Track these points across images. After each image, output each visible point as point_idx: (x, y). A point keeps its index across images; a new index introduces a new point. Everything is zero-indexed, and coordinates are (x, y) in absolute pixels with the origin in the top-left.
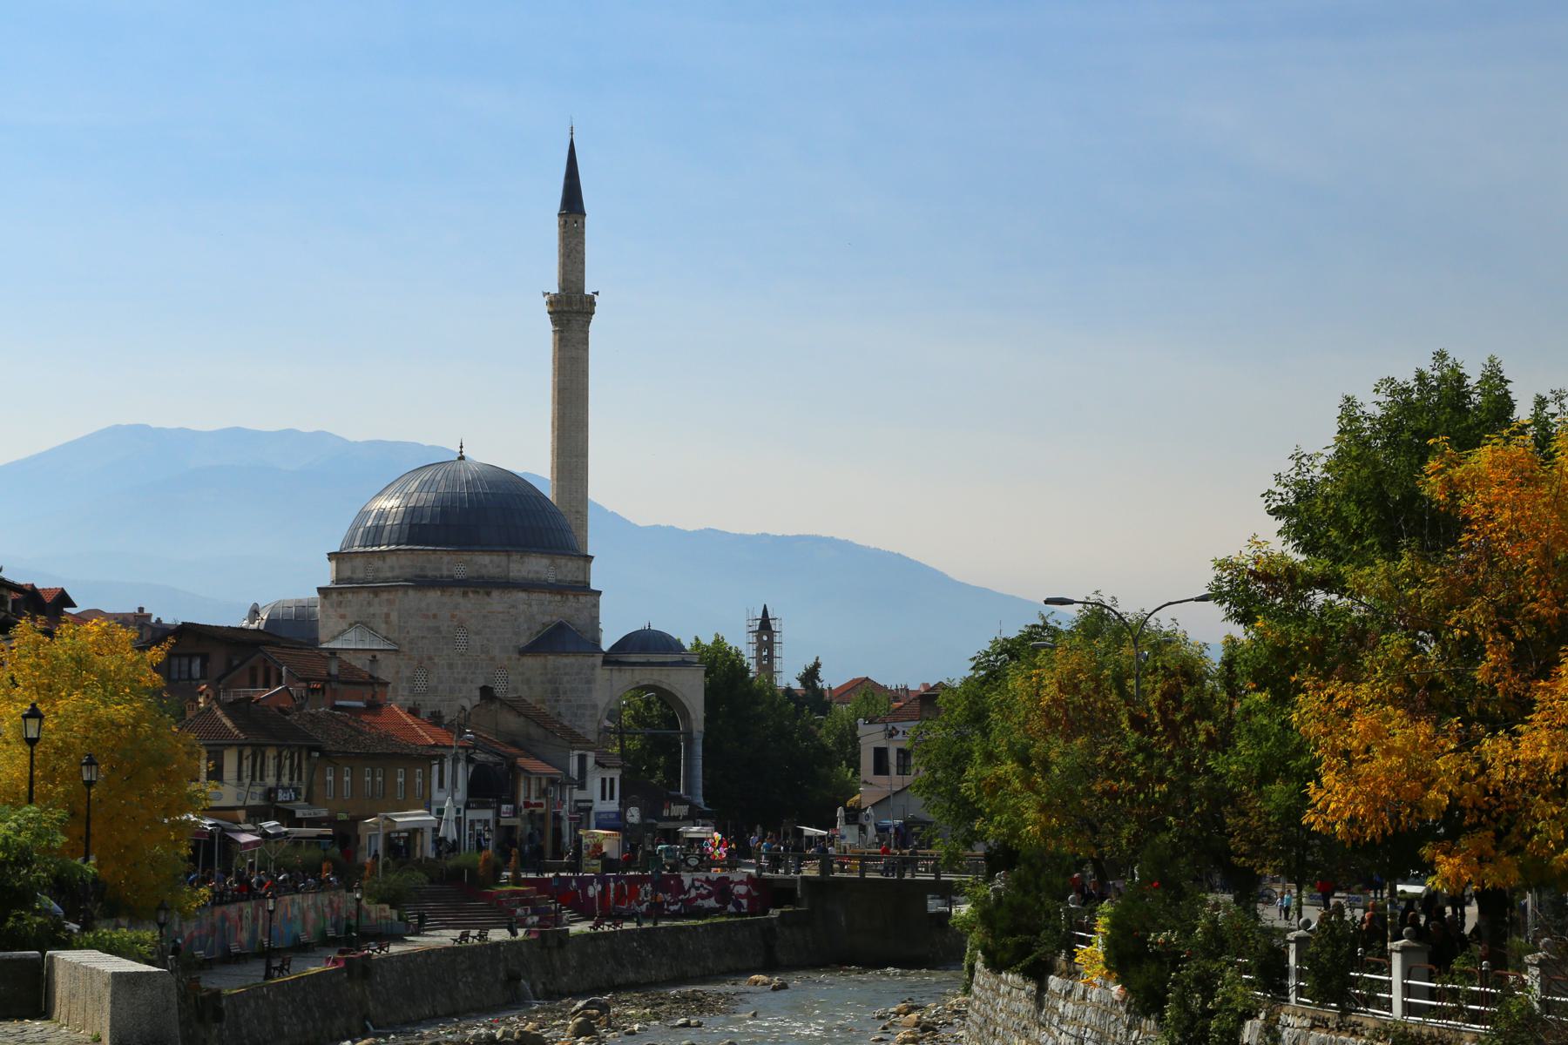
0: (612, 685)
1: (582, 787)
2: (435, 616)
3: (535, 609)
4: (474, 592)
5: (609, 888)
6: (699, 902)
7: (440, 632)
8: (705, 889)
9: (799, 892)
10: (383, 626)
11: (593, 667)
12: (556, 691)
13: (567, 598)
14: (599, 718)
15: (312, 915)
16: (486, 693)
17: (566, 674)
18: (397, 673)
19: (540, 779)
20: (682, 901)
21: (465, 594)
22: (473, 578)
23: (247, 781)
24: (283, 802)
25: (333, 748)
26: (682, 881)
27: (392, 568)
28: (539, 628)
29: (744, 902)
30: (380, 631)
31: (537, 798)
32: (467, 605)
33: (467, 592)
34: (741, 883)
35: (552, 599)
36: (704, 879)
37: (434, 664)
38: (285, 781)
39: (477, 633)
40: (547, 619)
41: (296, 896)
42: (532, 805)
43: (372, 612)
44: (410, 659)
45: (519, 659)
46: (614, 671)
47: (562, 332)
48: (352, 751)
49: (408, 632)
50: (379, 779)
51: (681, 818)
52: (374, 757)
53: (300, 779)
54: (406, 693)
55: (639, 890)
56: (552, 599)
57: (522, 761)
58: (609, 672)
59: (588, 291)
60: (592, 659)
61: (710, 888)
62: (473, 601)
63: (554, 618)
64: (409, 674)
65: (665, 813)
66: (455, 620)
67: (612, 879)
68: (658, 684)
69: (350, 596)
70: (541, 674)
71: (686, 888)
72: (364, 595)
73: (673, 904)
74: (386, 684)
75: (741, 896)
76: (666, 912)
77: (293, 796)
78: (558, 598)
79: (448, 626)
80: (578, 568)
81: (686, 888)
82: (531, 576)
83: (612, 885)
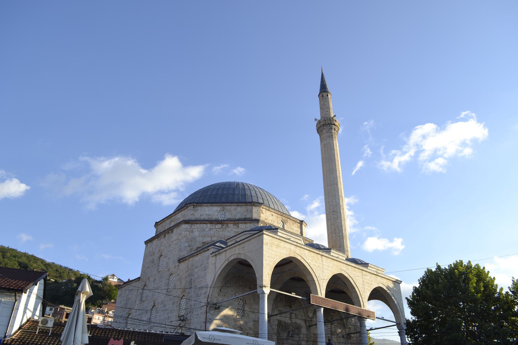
0: (216, 267)
7: (153, 262)
12: (190, 282)
13: (228, 226)
17: (197, 267)
33: (166, 234)
35: (212, 227)
39: (166, 257)
40: (207, 239)
46: (217, 256)
56: (213, 227)
58: (215, 257)
60: (208, 252)
62: (167, 239)
63: (215, 239)
66: (159, 252)
68: (239, 257)
70: (186, 272)
78: (220, 226)
80: (247, 210)
82: (202, 218)
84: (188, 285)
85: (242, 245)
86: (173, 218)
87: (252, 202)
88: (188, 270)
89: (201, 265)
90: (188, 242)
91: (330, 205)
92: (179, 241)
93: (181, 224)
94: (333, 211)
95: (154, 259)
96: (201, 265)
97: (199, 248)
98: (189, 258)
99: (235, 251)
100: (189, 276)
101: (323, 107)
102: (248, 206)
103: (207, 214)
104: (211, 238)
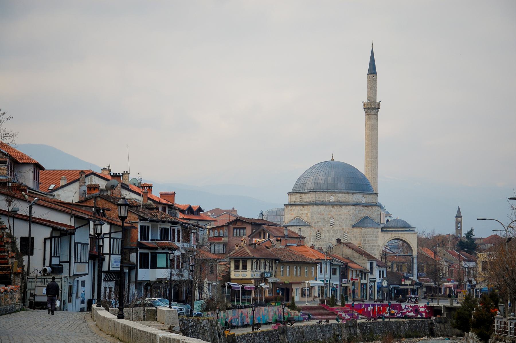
1: (372, 273)
2: (323, 214)
3: (357, 212)
4: (336, 206)
5: (375, 308)
6: (408, 314)
7: (325, 220)
8: (410, 309)
9: (443, 311)
10: (306, 218)
11: (378, 232)
12: (365, 240)
14: (380, 250)
15: (272, 313)
16: (339, 241)
18: (311, 234)
19: (356, 270)
20: (401, 313)
21: (333, 207)
22: (336, 201)
23: (254, 270)
24: (267, 277)
25: (283, 260)
26: (402, 306)
27: (309, 198)
28: (359, 219)
29: (424, 314)
30: (304, 220)
31: (355, 277)
32: (334, 211)
34: (422, 307)
35: (363, 208)
36: (409, 306)
37: (323, 231)
38: (267, 270)
39: (338, 220)
40: (362, 215)
41: (266, 307)
42: (353, 280)
43: (302, 213)
44: (315, 229)
45: (352, 229)
47: (368, 115)
48: (289, 261)
49: (314, 220)
50: (299, 270)
51: (409, 285)
52: (297, 263)
53: (272, 270)
54: (314, 241)
55: (386, 309)
56: (363, 208)
57: (349, 264)
59: (378, 101)
60: (377, 229)
61: (412, 309)
64: (314, 234)
65: (403, 283)
67: (376, 305)
69: (295, 207)
70: (360, 234)
71: (403, 309)
72: (299, 207)
73: (398, 314)
74: (304, 238)
75: (422, 312)
76: (396, 317)
77: (270, 275)
78: (366, 208)
79: (328, 218)
80: (373, 198)
81: (403, 309)
82: (356, 201)
83: (376, 307)
84: (363, 242)
85: (404, 234)
86: (333, 194)
87: (376, 194)
88: (361, 234)
89: (372, 234)
90: (354, 216)
91: (372, 172)
92: (350, 215)
93: (350, 205)
94: (374, 178)
95: (324, 218)
96: (372, 234)
97: (359, 220)
98: (361, 228)
99: (398, 235)
100: (363, 237)
101: (373, 89)
102: (373, 195)
103: (357, 199)
104: (363, 214)
